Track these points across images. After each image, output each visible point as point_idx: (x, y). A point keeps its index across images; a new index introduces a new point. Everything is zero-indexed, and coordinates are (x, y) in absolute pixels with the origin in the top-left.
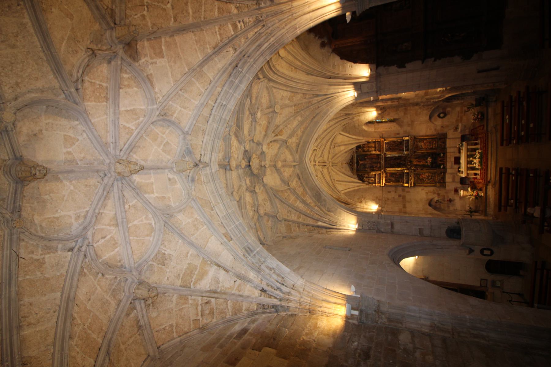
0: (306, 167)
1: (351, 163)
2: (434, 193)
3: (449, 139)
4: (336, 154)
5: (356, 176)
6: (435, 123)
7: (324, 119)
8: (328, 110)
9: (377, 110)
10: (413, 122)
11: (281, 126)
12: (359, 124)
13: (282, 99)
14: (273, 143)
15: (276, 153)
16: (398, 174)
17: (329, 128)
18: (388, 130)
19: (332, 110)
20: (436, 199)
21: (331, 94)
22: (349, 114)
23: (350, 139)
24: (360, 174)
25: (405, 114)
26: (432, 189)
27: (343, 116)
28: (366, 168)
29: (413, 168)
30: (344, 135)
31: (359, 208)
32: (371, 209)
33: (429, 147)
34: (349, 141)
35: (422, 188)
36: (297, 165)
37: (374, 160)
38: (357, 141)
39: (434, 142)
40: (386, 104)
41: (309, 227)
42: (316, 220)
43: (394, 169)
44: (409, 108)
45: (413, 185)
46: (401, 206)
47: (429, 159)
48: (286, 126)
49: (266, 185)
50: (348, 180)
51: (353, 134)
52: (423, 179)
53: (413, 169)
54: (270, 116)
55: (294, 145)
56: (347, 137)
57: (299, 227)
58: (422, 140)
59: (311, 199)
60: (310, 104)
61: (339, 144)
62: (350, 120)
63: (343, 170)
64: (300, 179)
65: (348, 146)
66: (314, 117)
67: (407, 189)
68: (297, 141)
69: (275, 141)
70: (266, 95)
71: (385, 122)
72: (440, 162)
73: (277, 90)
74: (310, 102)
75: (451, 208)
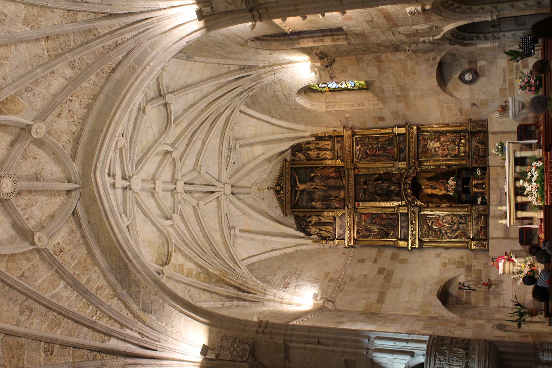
0: (97, 195)
1: (278, 188)
2: (460, 264)
3: (494, 133)
4: (244, 165)
5: (291, 220)
6: (457, 94)
7: (137, 73)
8: (145, 53)
9: (312, 59)
10: (404, 90)
11: (7, 89)
12: (285, 92)
16: (384, 217)
17: (201, 99)
18: (356, 108)
19: (153, 54)
20: (461, 279)
21: (142, 12)
22: (250, 68)
23: (275, 128)
24: (301, 215)
25: (380, 71)
26: (456, 254)
27: (235, 71)
28: (313, 200)
29: (419, 203)
30: (258, 119)
31: (270, 301)
32: (299, 305)
33: (453, 153)
34: (273, 133)
35: (438, 251)
36: (76, 189)
37: (332, 182)
38: (292, 135)
39: (462, 141)
40: (321, 44)
41: (79, 352)
42: (105, 334)
43: (376, 204)
44: (384, 57)
45: (416, 245)
46: (374, 296)
47: (451, 182)
48: (28, 90)
50: (273, 230)
51: (281, 118)
52: (440, 231)
53: (420, 207)
55: (65, 137)
56: (267, 124)
57: (49, 352)
58: (438, 135)
59: (105, 277)
60: (91, 36)
61: (249, 141)
62: (253, 80)
63: (264, 206)
64: (80, 226)
65: (271, 146)
66: (114, 70)
67: (403, 255)
68: (74, 129)
71: (347, 89)
72: (476, 190)
74: (90, 31)
75: (493, 304)
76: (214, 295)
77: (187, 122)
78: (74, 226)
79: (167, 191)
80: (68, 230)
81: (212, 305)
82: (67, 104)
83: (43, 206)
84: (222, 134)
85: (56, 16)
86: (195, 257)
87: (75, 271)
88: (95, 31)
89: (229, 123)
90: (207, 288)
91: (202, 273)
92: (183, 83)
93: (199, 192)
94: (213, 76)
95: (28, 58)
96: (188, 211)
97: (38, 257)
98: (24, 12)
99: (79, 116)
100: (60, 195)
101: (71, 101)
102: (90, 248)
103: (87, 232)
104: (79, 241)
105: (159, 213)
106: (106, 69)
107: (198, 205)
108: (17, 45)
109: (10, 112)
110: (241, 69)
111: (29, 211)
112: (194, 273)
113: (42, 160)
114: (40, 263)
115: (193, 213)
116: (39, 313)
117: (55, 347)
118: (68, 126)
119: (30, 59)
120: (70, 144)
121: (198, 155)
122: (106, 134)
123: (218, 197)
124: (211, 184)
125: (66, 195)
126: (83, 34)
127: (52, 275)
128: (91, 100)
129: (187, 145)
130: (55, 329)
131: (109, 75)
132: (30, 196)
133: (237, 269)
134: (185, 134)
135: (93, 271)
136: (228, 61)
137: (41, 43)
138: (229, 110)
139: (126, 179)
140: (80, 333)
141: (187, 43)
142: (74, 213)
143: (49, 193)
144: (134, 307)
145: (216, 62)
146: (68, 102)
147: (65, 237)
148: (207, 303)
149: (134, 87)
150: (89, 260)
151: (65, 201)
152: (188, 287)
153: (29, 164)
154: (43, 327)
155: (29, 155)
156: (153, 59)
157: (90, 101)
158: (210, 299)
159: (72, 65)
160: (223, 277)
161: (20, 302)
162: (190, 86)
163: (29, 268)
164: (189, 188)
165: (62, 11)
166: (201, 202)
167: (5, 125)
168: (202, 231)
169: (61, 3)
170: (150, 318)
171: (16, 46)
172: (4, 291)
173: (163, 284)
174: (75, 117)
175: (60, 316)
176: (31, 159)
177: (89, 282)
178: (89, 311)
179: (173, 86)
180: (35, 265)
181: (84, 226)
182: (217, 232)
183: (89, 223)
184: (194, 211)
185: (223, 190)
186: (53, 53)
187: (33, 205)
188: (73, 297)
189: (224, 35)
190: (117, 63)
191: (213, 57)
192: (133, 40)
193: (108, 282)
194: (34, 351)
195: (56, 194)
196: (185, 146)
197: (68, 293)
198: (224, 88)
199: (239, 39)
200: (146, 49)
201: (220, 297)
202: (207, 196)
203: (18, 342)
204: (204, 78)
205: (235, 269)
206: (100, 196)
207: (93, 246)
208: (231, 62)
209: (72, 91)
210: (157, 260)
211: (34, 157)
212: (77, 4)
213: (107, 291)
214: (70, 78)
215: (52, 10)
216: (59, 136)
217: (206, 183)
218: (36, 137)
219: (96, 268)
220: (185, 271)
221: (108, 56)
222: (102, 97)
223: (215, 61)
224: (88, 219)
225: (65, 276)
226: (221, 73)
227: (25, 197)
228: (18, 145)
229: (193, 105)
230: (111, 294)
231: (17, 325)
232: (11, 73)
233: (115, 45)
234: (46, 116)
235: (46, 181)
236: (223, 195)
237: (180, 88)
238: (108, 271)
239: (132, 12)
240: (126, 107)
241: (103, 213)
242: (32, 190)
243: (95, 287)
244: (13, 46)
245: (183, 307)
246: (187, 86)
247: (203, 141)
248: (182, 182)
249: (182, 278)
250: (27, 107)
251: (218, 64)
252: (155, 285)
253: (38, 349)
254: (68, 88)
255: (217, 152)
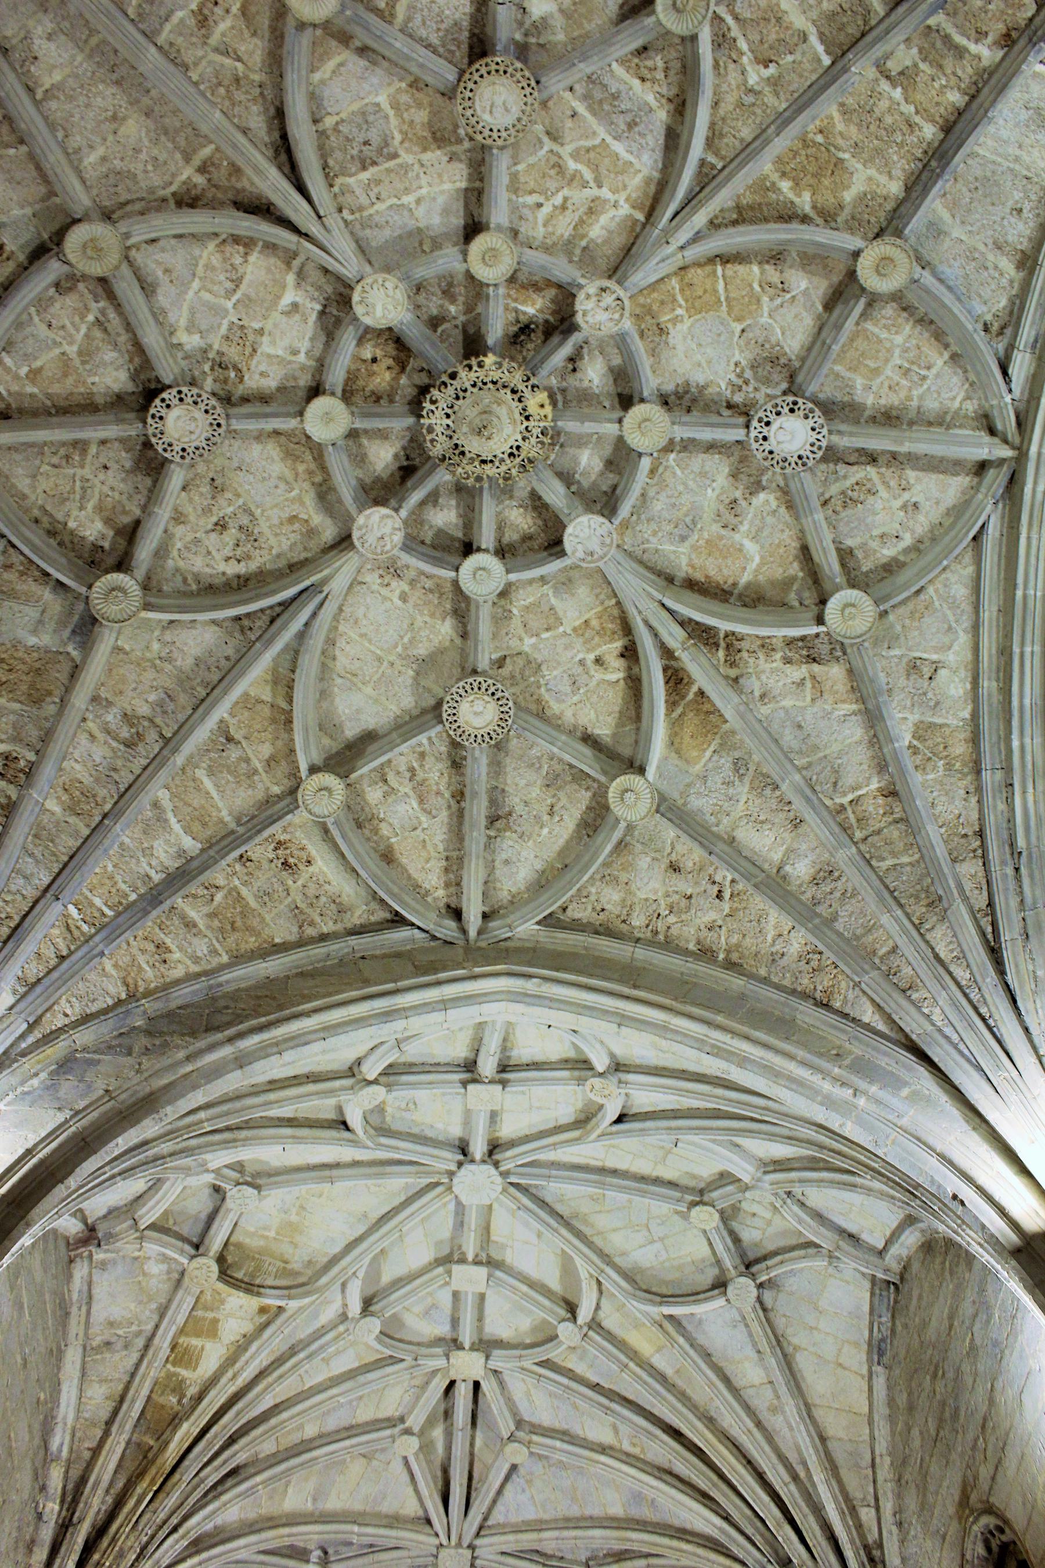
13: (914, 667)
14: (616, 672)
15: (555, 707)
27: (859, 1526)
36: (464, 931)
48: (739, 766)
49: (352, 546)
54: (792, 598)
55: (611, 897)
59: (190, 977)
60: (918, 910)
68: (638, 921)
69: (635, 685)
70: (922, 524)
73: (967, 607)
76: (99, 1433)
77: (669, 1372)
78: (358, 917)
79: (455, 1322)
80: (345, 899)
81: (65, 1418)
82: (709, 886)
83: (418, 832)
84: (638, 1522)
85: (957, 806)
86: (234, 1377)
87: (225, 891)
88: (935, 918)
89: (675, 1543)
90: (125, 1407)
91: (179, 1402)
92: (795, 1341)
93: (448, 1448)
94: (829, 1444)
95: (827, 752)
96: (389, 1408)
97: (276, 790)
98: (953, 721)
99: (674, 931)
100: (447, 885)
101: (719, 896)
102: (286, 950)
103: (335, 948)
104: (312, 924)
105: (386, 1278)
106: (824, 982)
107: (408, 1432)
108: (859, 717)
109: (675, 726)
110: (866, 1547)
111: (406, 788)
112: (184, 1373)
113: (545, 831)
114: (260, 795)
115: (381, 1415)
116: (119, 763)
117: (12, 787)
118: (646, 900)
119: (825, 757)
120: (595, 914)
121: (565, 1433)
122: (627, 998)
123: (429, 1522)
124: (473, 1494)
125: (448, 906)
126: (918, 887)
127: (221, 821)
128: (726, 959)
129: (596, 1387)
130: (65, 797)
131: (805, 996)
132: (447, 795)
133: (177, 1541)
134: (632, 1365)
135: (217, 945)
136: (890, 1495)
137: (875, 780)
138: (720, 1529)
139: (491, 1153)
140: (37, 862)
141: (955, 1197)
142: (398, 920)
143: (455, 854)
144: (84, 1037)
145: (877, 1452)
146: (716, 888)
147: (327, 887)
148: (74, 1400)
149: (778, 1061)
150: (252, 943)
151: (429, 899)
152: (140, 1342)
153: (534, 795)
154: (77, 767)
155: (561, 794)
156: (878, 1102)
157: (721, 956)
158: (87, 1415)
159: (827, 873)
160: (153, 1471)
161: (158, 720)
162: (788, 1363)
163: (247, 760)
164: (463, 1394)
165: (975, 815)
166: (414, 1443)
167: (638, 718)
168: (321, 1436)
169: (999, 803)
170: (36, 1075)
171: (854, 713)
172: (195, 683)
173: (138, 1121)
174: (672, 919)
175: (98, 819)
176: (549, 802)
177: (187, 925)
178: (98, 902)
179: (780, 1303)
180: (256, 778)
181: (354, 941)
182: (315, 1500)
183: (363, 958)
184: (388, 1419)
185: (453, 1543)
186: (852, 816)
187: (421, 801)
188: (148, 868)
189: (992, 1402)
190: (846, 1010)
191: (893, 1433)
192: (930, 1028)
193: (177, 982)
194: (14, 728)
195: (452, 876)
196: (594, 1379)
197: (163, 856)
198: (793, 1487)
199: (985, 1472)
200: (906, 1084)
201: (87, 1455)
202: (434, 1477)
203: (49, 693)
204: (817, 1413)
205: (176, 1536)
206: (439, 983)
207: (294, 957)
208: (888, 1507)
209: (748, 880)
210: (239, 1246)
211: (555, 809)
212: (1007, 848)
213: (149, 973)
214: (784, 878)
215: (972, 789)
216: (616, 879)
217: (475, 1475)
218: (610, 795)
219: (225, 959)
220: (196, 1342)
221: (867, 967)
222: (738, 983)
223: (881, 1447)
224: (374, 957)
225: (212, 853)
226: (843, 1472)
227: (446, 779)
228: (587, 751)
229: (727, 1380)
230: (140, 983)
231: (95, 699)
232: (782, 714)
233: (903, 985)
234: (669, 815)
235: (487, 846)
236: (437, 1542)
237: (780, 1332)
238: (211, 987)
239: (1020, 1004)
240: (713, 1046)
241: (390, 986)
242: (463, 804)
243: (168, 941)
244: (854, 707)
245: (42, 1162)
246: (785, 1355)
247: (611, 1448)
248: (482, 1372)
249: (173, 1322)
250: (691, 770)
251: (873, 1460)
252: (141, 1095)
253: (16, 739)
254: (756, 871)
255: (575, 1511)
